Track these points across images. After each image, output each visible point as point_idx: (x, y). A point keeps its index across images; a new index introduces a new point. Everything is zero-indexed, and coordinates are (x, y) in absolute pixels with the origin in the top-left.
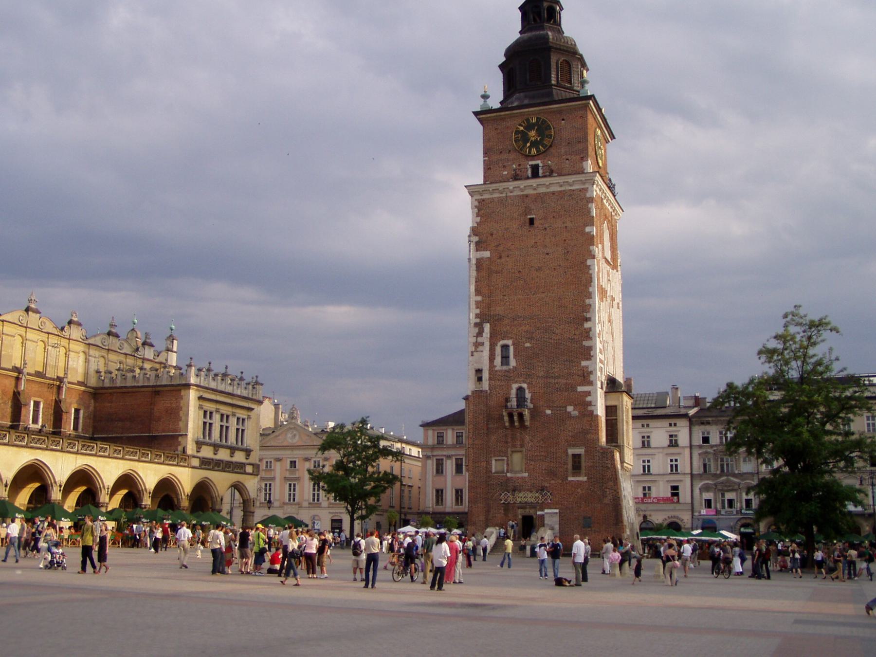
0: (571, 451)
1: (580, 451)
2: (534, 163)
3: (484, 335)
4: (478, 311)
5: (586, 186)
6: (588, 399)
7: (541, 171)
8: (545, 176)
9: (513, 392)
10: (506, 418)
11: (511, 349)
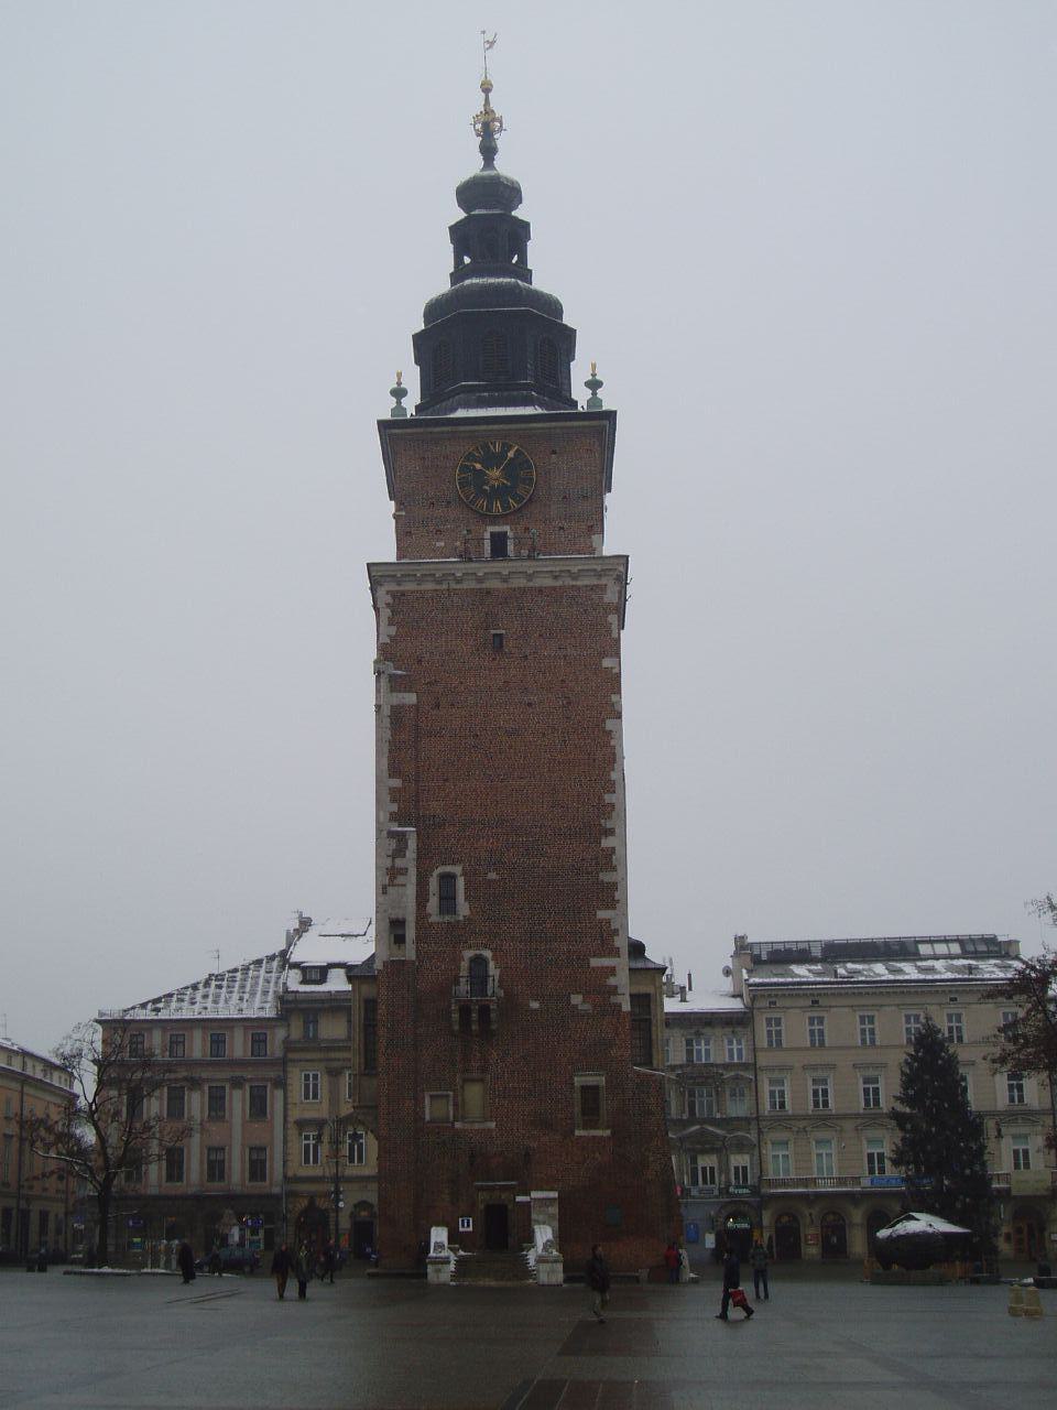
0: (578, 1081)
1: (601, 1080)
2: (497, 529)
4: (394, 807)
5: (603, 581)
6: (612, 981)
7: (510, 547)
8: (519, 558)
9: (465, 965)
10: (456, 1016)
11: (461, 883)
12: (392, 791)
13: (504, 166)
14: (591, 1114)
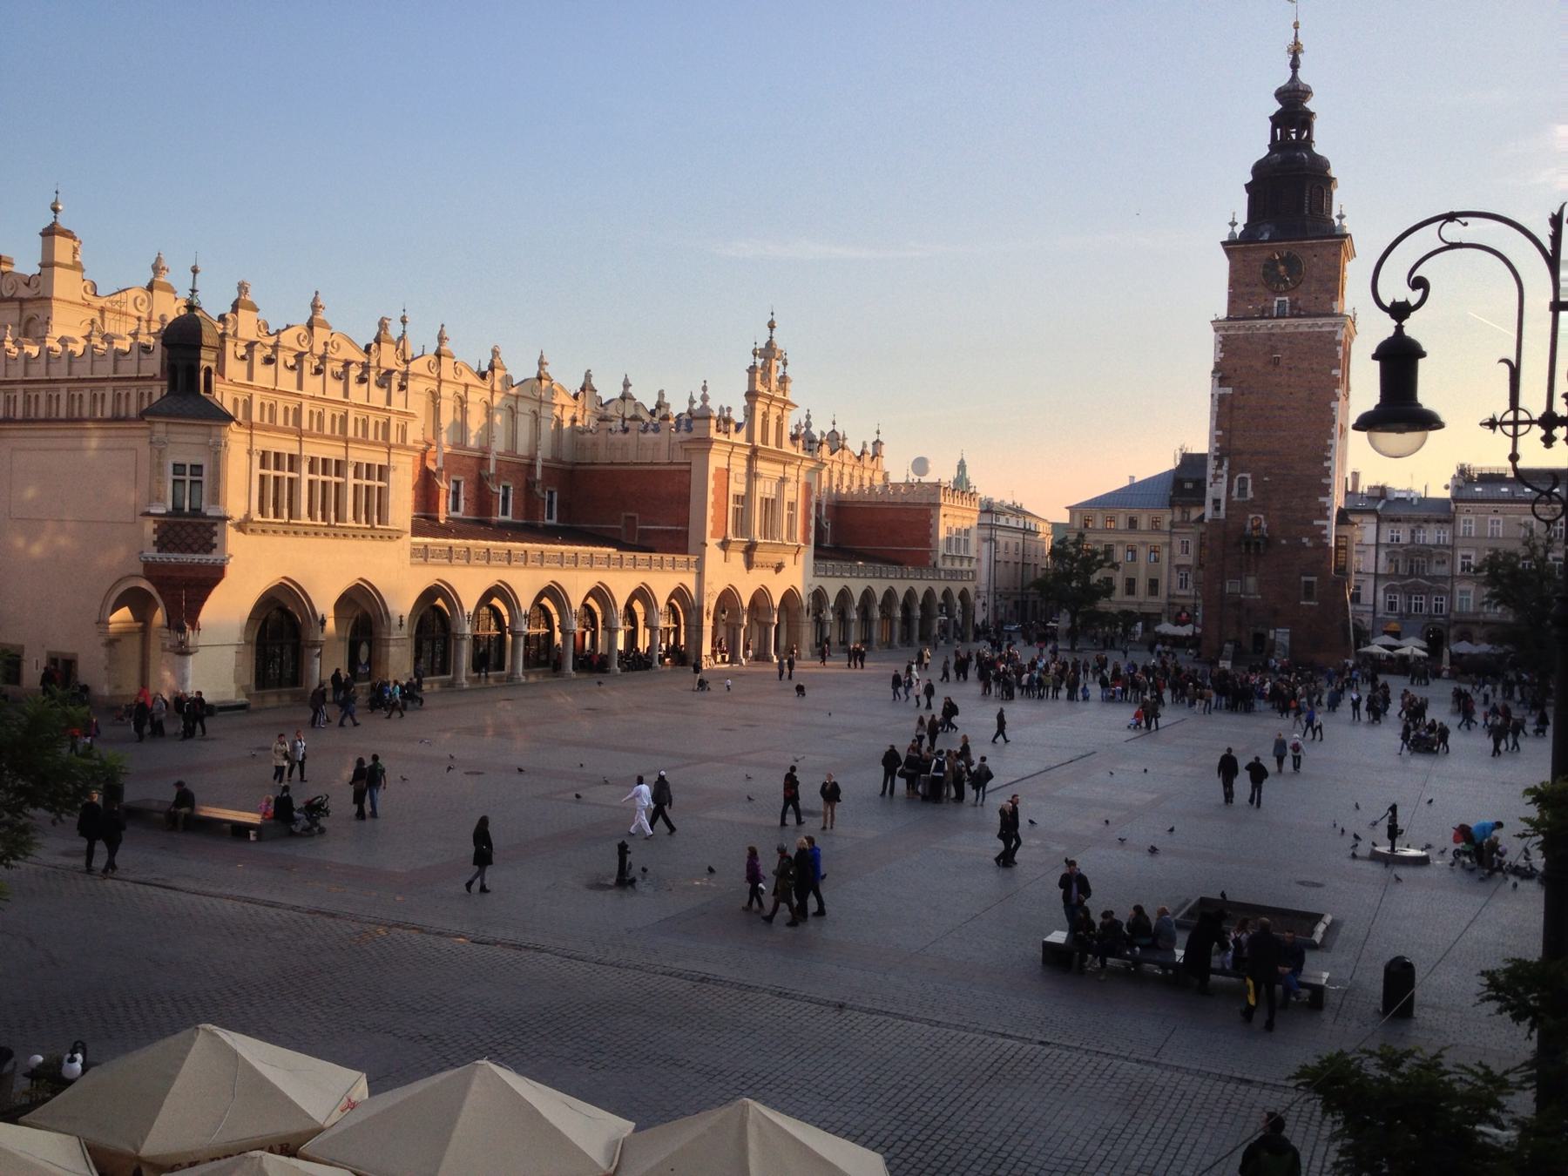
1: (1315, 579)
3: (1225, 468)
8: (1292, 316)
12: (1217, 437)
13: (1304, 76)
14: (1309, 596)
